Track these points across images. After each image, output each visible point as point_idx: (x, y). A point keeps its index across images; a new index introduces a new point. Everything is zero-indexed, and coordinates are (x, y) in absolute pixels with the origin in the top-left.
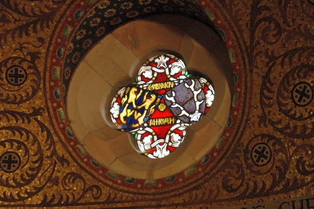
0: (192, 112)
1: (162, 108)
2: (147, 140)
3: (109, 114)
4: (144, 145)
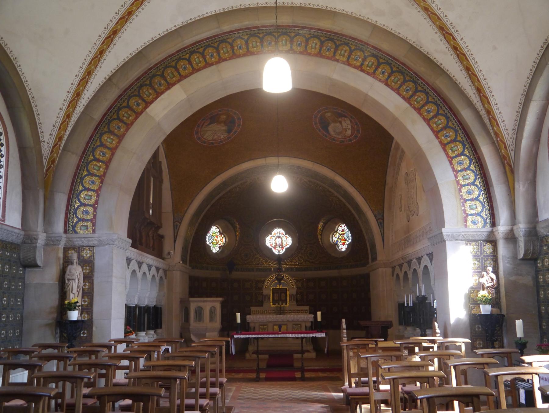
0: (349, 239)
1: (343, 238)
2: (341, 246)
3: (332, 240)
4: (340, 248)
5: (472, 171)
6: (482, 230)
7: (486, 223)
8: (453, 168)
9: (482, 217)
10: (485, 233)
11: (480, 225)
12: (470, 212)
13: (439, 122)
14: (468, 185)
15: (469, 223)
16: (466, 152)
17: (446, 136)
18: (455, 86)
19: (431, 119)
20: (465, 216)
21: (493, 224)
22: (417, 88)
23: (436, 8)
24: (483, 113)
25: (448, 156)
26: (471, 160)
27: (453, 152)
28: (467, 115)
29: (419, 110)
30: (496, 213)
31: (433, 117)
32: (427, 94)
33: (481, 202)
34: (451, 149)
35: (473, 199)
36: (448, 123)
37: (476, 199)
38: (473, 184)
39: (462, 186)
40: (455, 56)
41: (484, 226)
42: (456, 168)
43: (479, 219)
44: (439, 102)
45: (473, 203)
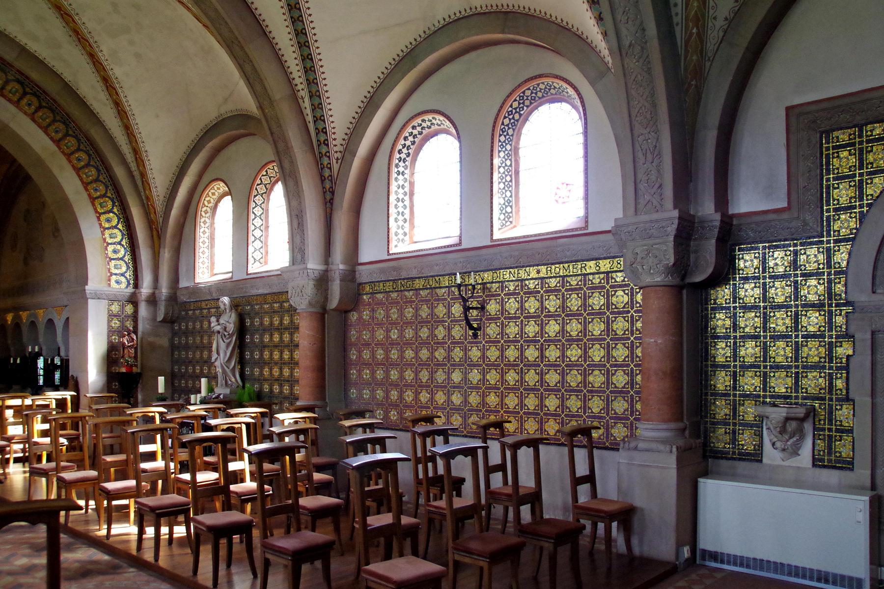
5: (120, 230)
6: (126, 290)
7: (129, 284)
8: (101, 225)
9: (126, 278)
10: (128, 294)
11: (123, 286)
12: (114, 271)
13: (90, 173)
14: (114, 244)
15: (113, 283)
16: (115, 210)
17: (96, 190)
18: (111, 139)
19: (81, 168)
20: (109, 274)
21: (136, 286)
22: (67, 131)
23: (103, 58)
24: (136, 174)
25: (96, 212)
26: (119, 219)
27: (102, 207)
28: (120, 173)
29: (68, 156)
30: (139, 275)
31: (83, 167)
32: (79, 140)
33: (126, 262)
34: (101, 204)
35: (118, 259)
36: (99, 176)
37: (122, 259)
38: (120, 243)
39: (108, 244)
40: (115, 111)
41: (127, 287)
42: (103, 225)
43: (123, 279)
44: (91, 152)
45: (118, 262)
